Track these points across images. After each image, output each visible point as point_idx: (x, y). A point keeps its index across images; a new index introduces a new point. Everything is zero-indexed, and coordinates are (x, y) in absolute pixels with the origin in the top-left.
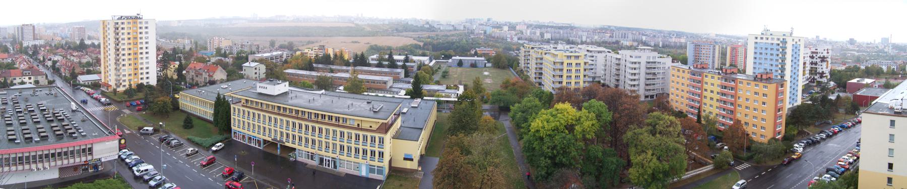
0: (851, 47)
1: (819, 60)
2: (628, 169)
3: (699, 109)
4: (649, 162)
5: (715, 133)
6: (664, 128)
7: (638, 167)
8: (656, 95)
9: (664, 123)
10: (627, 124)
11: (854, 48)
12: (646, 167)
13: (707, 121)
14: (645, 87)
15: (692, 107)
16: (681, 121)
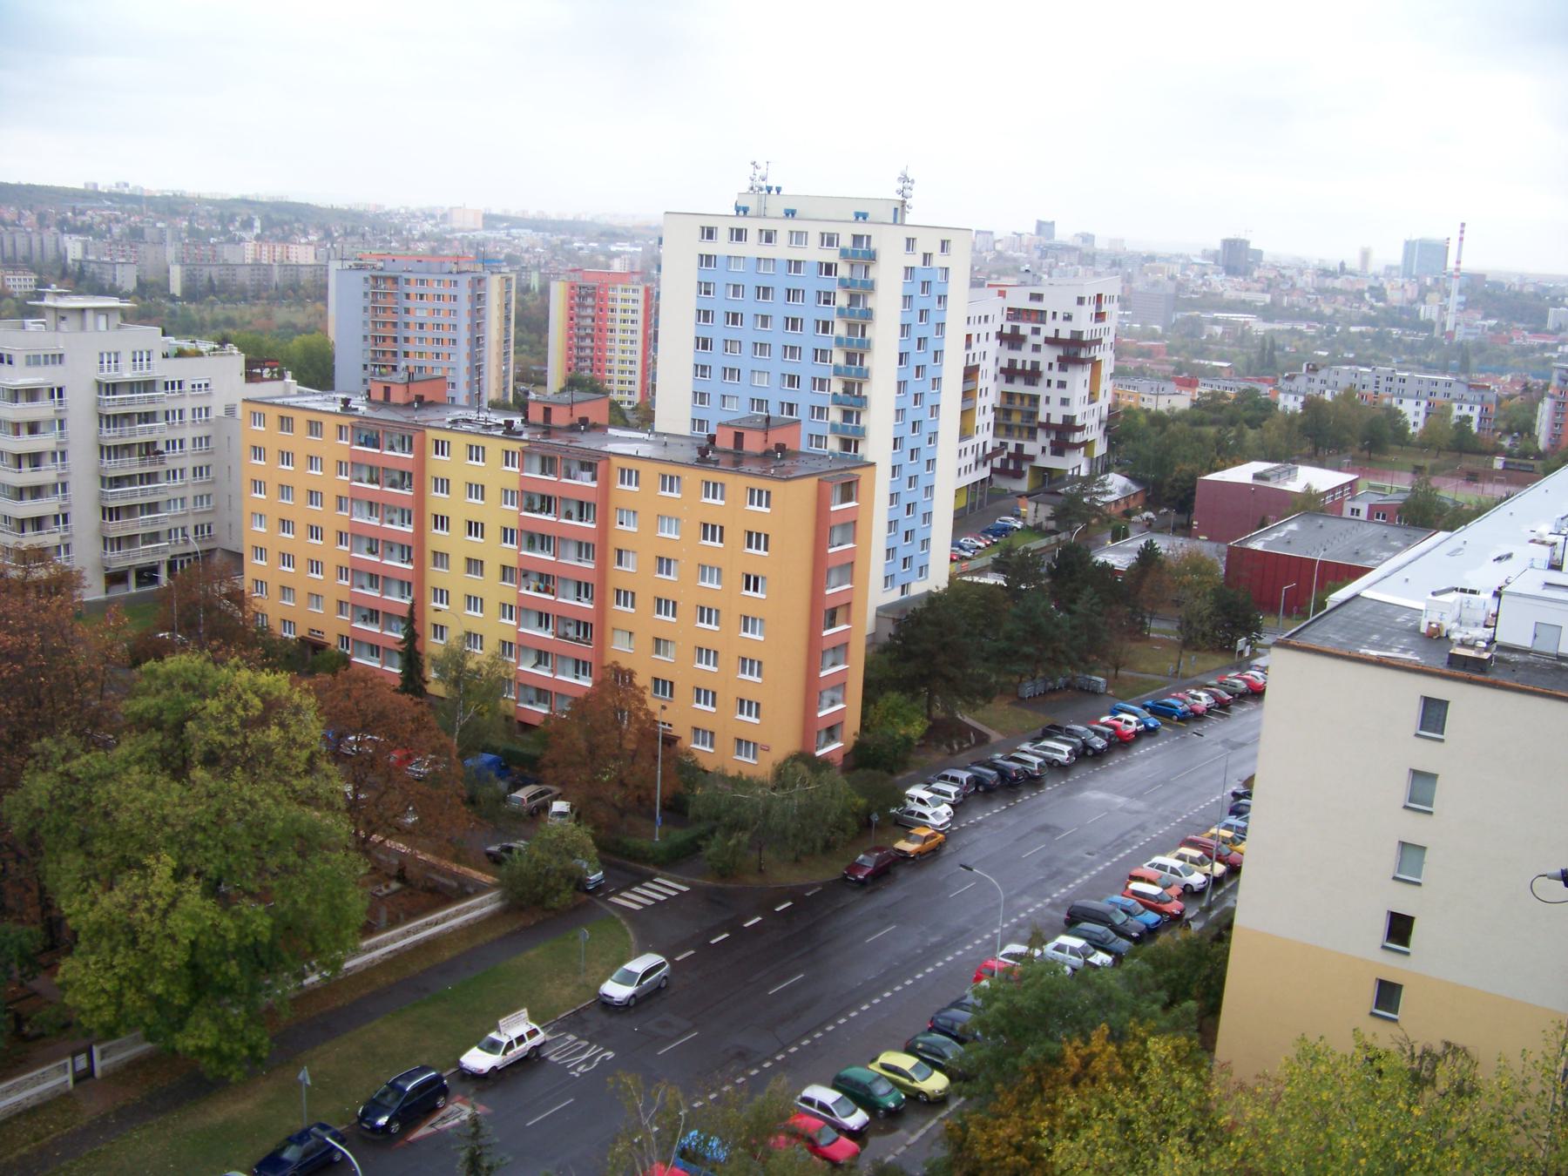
0: (1224, 286)
1: (1048, 356)
2: (52, 968)
3: (411, 621)
4: (165, 913)
5: (500, 741)
6: (230, 732)
7: (105, 944)
8: (171, 566)
9: (230, 709)
10: (19, 737)
11: (1244, 296)
12: (152, 941)
13: (456, 682)
14: (101, 530)
15: (372, 616)
16: (319, 693)
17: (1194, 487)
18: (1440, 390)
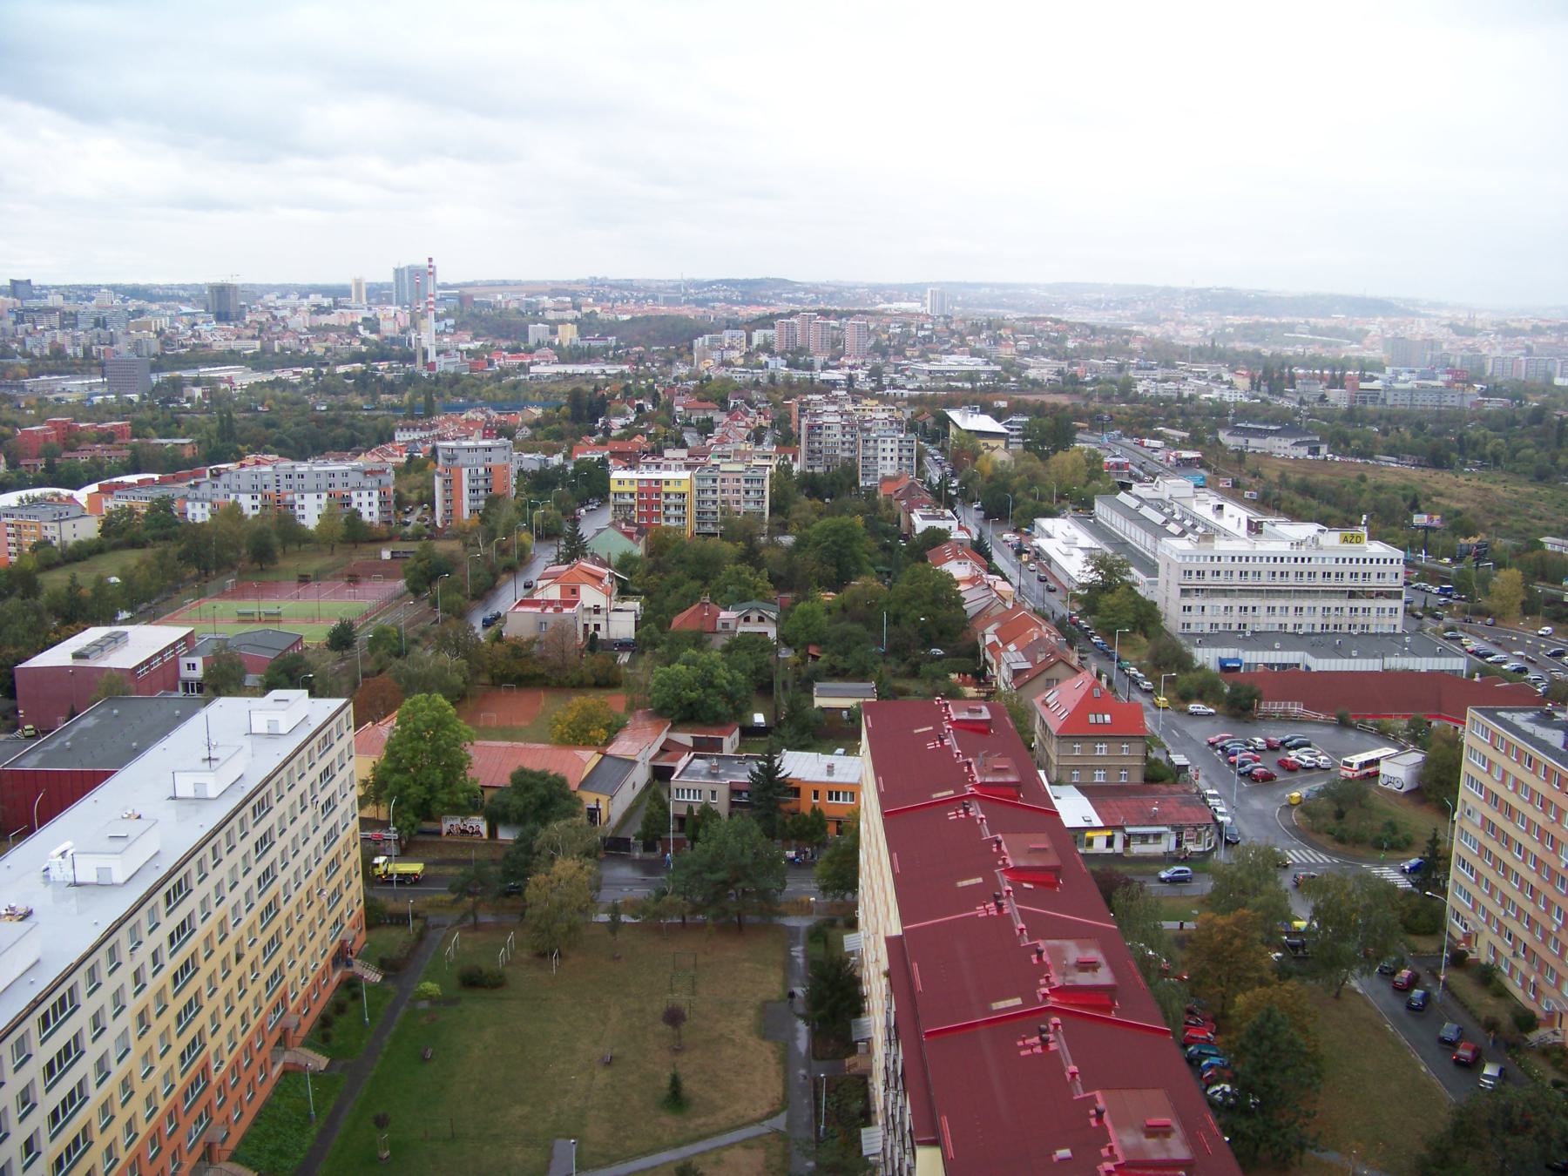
17: (12, 676)
18: (339, 480)
